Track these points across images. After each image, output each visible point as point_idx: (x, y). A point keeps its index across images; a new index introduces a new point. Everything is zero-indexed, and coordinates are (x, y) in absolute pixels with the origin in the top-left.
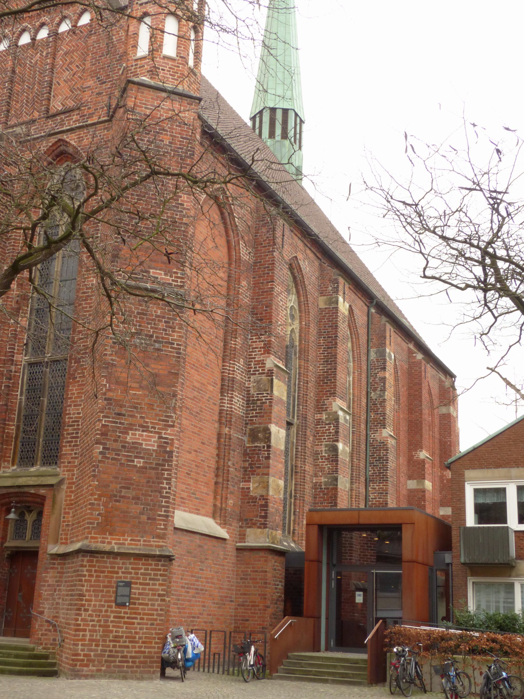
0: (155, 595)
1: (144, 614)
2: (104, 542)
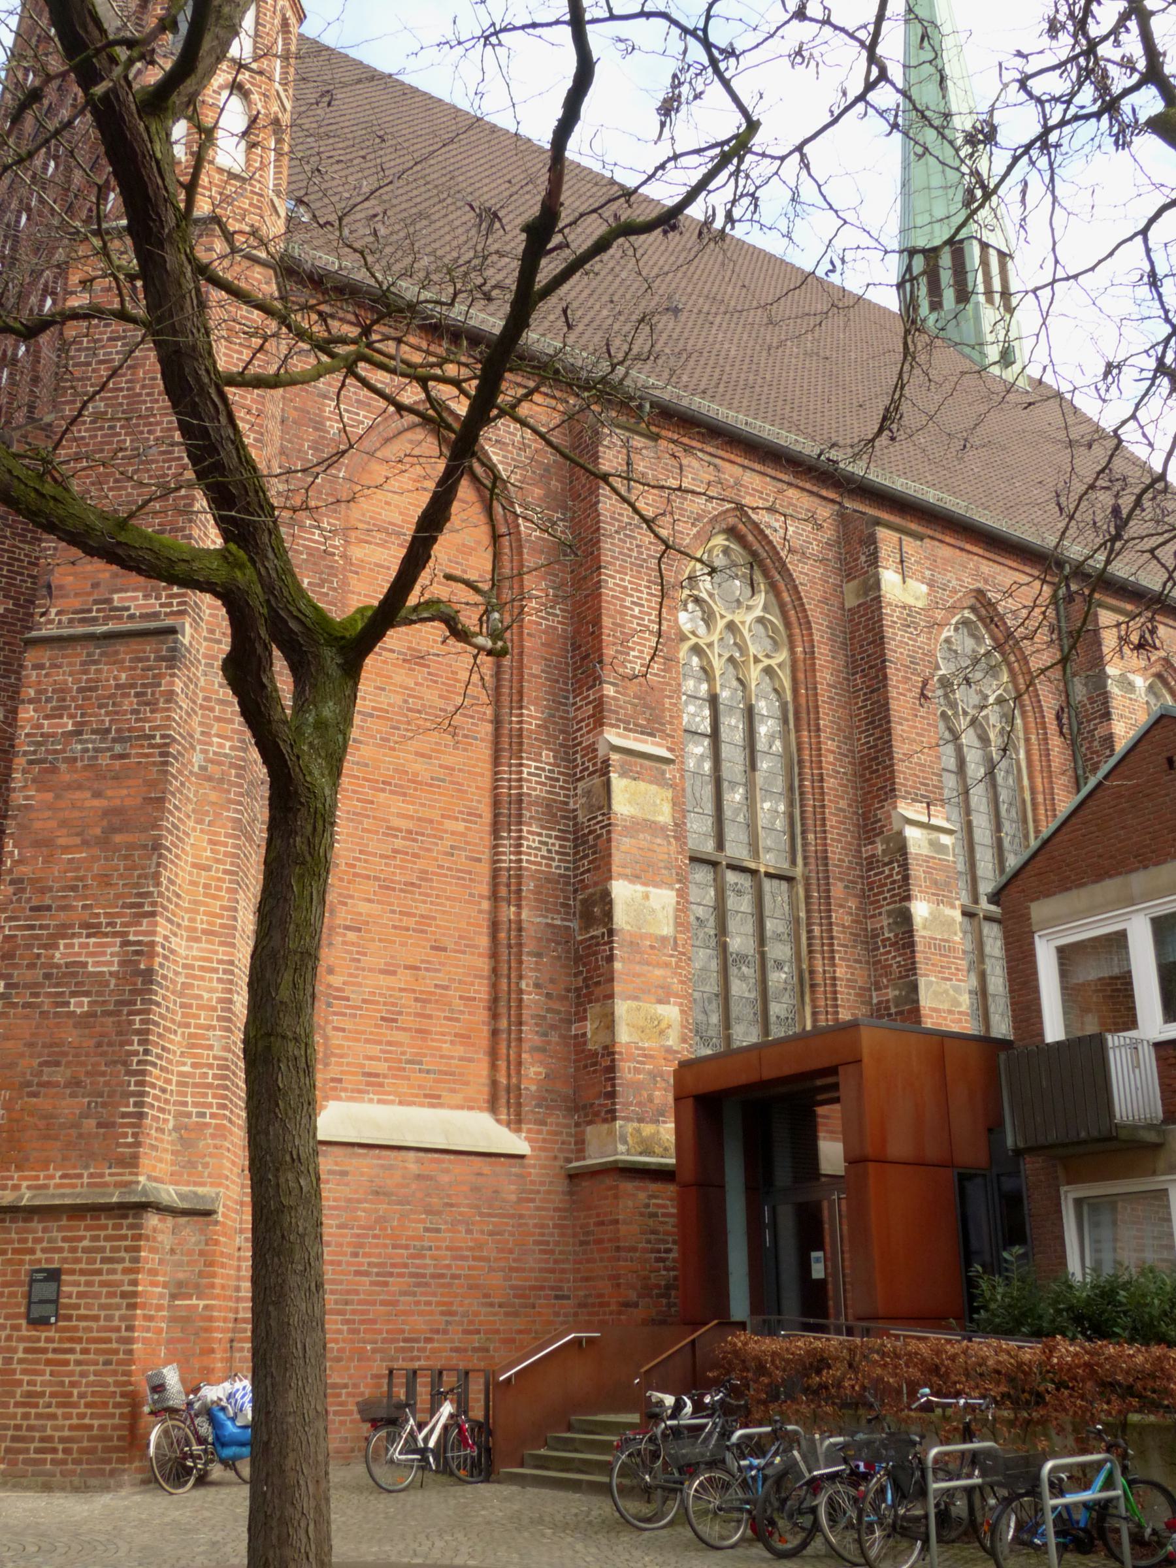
0: (111, 1295)
1: (90, 1341)
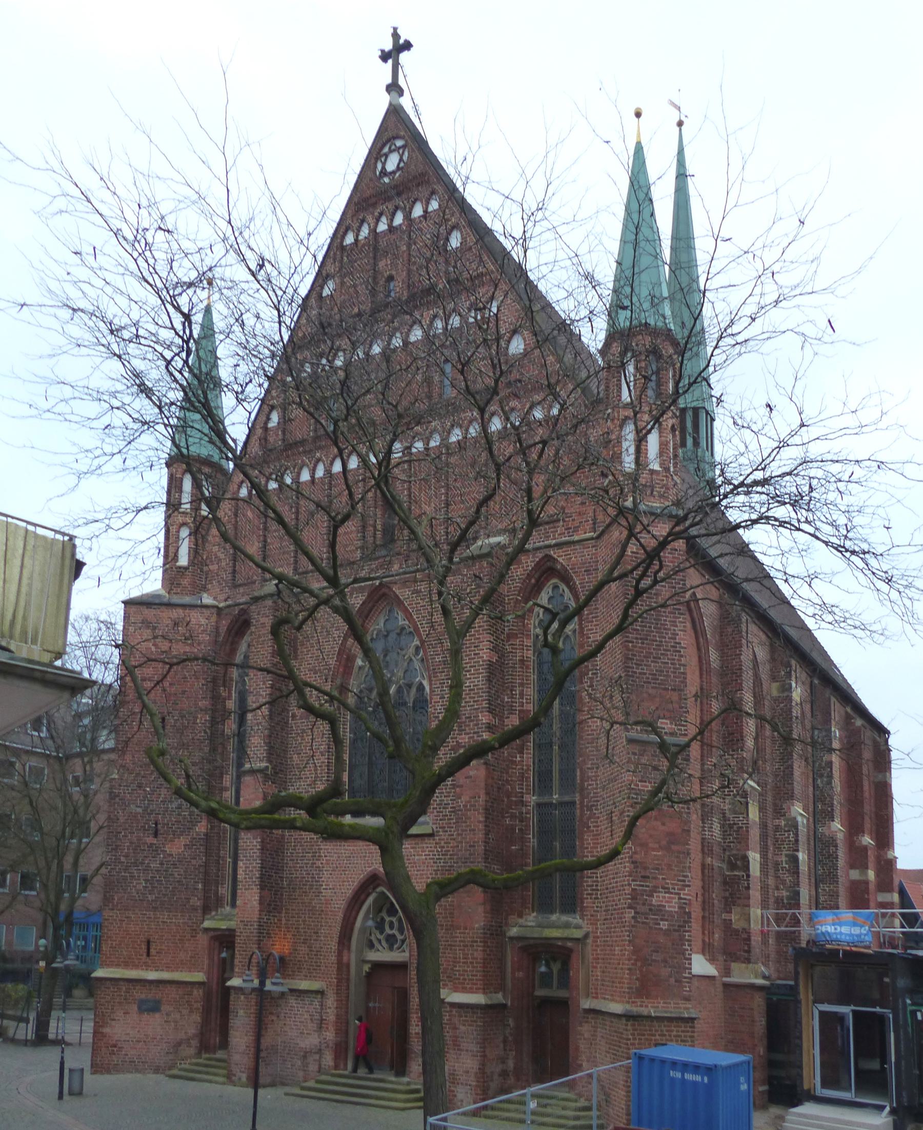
2: (641, 1006)
